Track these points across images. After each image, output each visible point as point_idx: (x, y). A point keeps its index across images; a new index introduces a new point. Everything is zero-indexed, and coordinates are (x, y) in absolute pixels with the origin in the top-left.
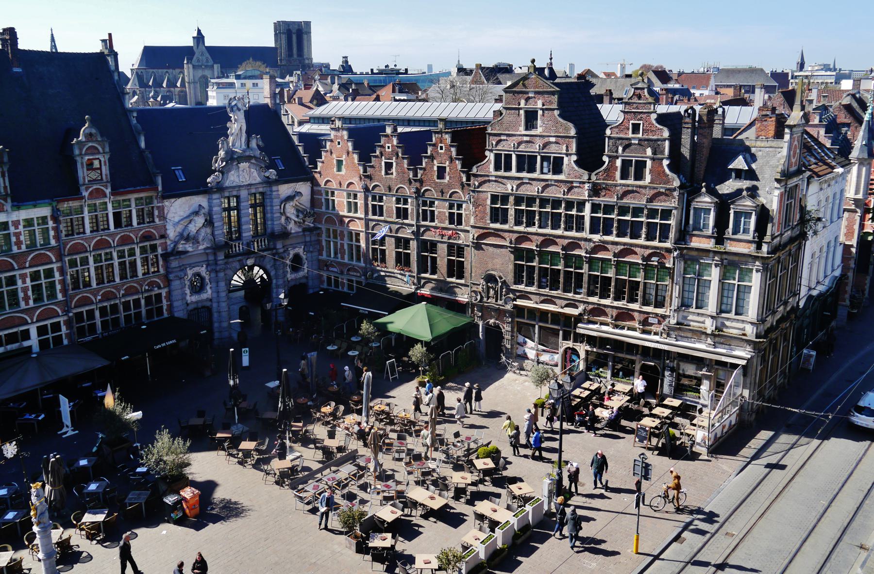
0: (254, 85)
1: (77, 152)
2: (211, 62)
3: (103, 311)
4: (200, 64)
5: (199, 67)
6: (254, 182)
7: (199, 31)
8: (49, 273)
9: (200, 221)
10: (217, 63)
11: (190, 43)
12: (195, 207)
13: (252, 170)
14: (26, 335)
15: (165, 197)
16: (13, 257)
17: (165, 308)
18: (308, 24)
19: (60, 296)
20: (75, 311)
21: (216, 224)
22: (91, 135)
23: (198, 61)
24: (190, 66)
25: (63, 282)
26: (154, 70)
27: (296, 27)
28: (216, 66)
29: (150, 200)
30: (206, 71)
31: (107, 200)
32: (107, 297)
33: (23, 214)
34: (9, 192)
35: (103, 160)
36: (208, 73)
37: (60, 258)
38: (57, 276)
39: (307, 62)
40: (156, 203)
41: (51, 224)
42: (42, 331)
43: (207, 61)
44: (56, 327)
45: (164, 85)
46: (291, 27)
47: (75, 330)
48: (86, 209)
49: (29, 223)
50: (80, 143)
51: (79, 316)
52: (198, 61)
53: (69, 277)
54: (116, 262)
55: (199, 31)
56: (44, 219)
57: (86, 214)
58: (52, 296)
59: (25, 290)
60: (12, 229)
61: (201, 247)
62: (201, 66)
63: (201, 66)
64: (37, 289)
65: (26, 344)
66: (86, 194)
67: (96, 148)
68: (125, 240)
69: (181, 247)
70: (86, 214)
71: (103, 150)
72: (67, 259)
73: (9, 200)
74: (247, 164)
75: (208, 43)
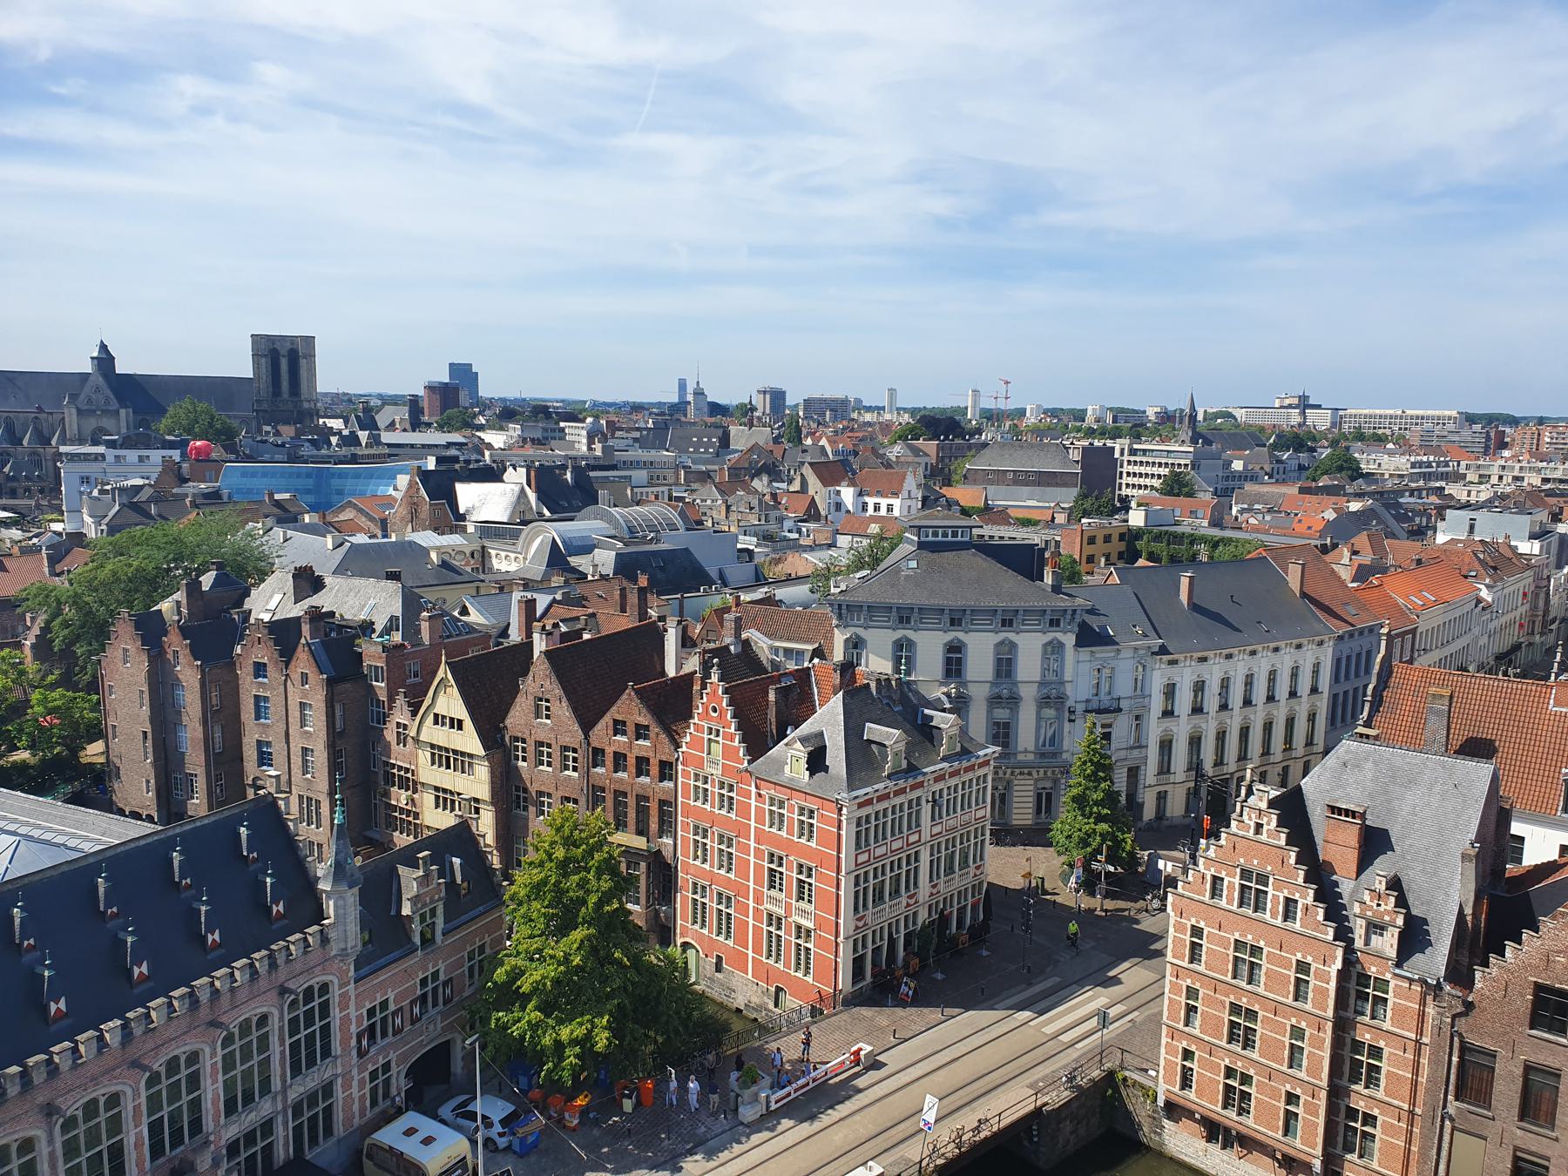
0: (141, 459)
2: (114, 404)
4: (93, 408)
5: (91, 412)
7: (103, 347)
10: (126, 407)
11: (87, 367)
18: (309, 341)
23: (90, 401)
24: (74, 411)
26: (11, 415)
27: (288, 345)
28: (123, 412)
30: (105, 420)
36: (107, 423)
39: (306, 405)
43: (107, 402)
45: (25, 443)
46: (277, 346)
52: (90, 401)
55: (103, 347)
62: (95, 411)
63: (95, 411)
75: (121, 368)
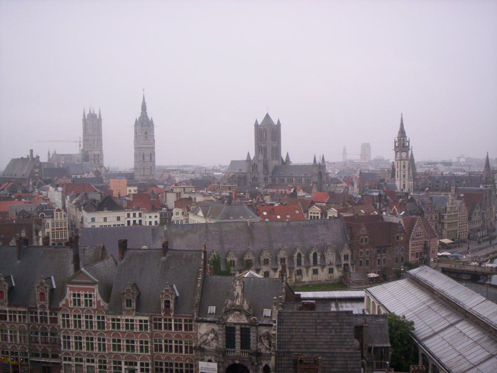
1: (161, 296)
3: (166, 364)
6: (242, 322)
8: (147, 342)
9: (212, 335)
12: (210, 329)
13: (243, 316)
14: (136, 364)
15: (198, 321)
16: (134, 333)
17: (194, 371)
19: (149, 353)
20: (155, 361)
21: (219, 339)
22: (167, 290)
25: (152, 348)
29: (191, 321)
31: (171, 317)
32: (169, 358)
33: (139, 318)
34: (135, 308)
35: (170, 300)
37: (151, 338)
38: (149, 345)
40: (193, 323)
41: (149, 323)
42: (142, 364)
44: (147, 365)
47: (154, 368)
48: (163, 320)
49: (141, 321)
50: (163, 294)
51: (157, 363)
53: (154, 346)
54: (174, 344)
56: (146, 321)
57: (163, 322)
58: (147, 351)
59: (137, 346)
60: (135, 322)
61: (211, 348)
64: (141, 347)
65: (136, 368)
66: (163, 314)
67: (168, 296)
68: (178, 336)
69: (202, 346)
70: (163, 322)
71: (172, 296)
72: (153, 339)
73: (135, 312)
74: (238, 313)
